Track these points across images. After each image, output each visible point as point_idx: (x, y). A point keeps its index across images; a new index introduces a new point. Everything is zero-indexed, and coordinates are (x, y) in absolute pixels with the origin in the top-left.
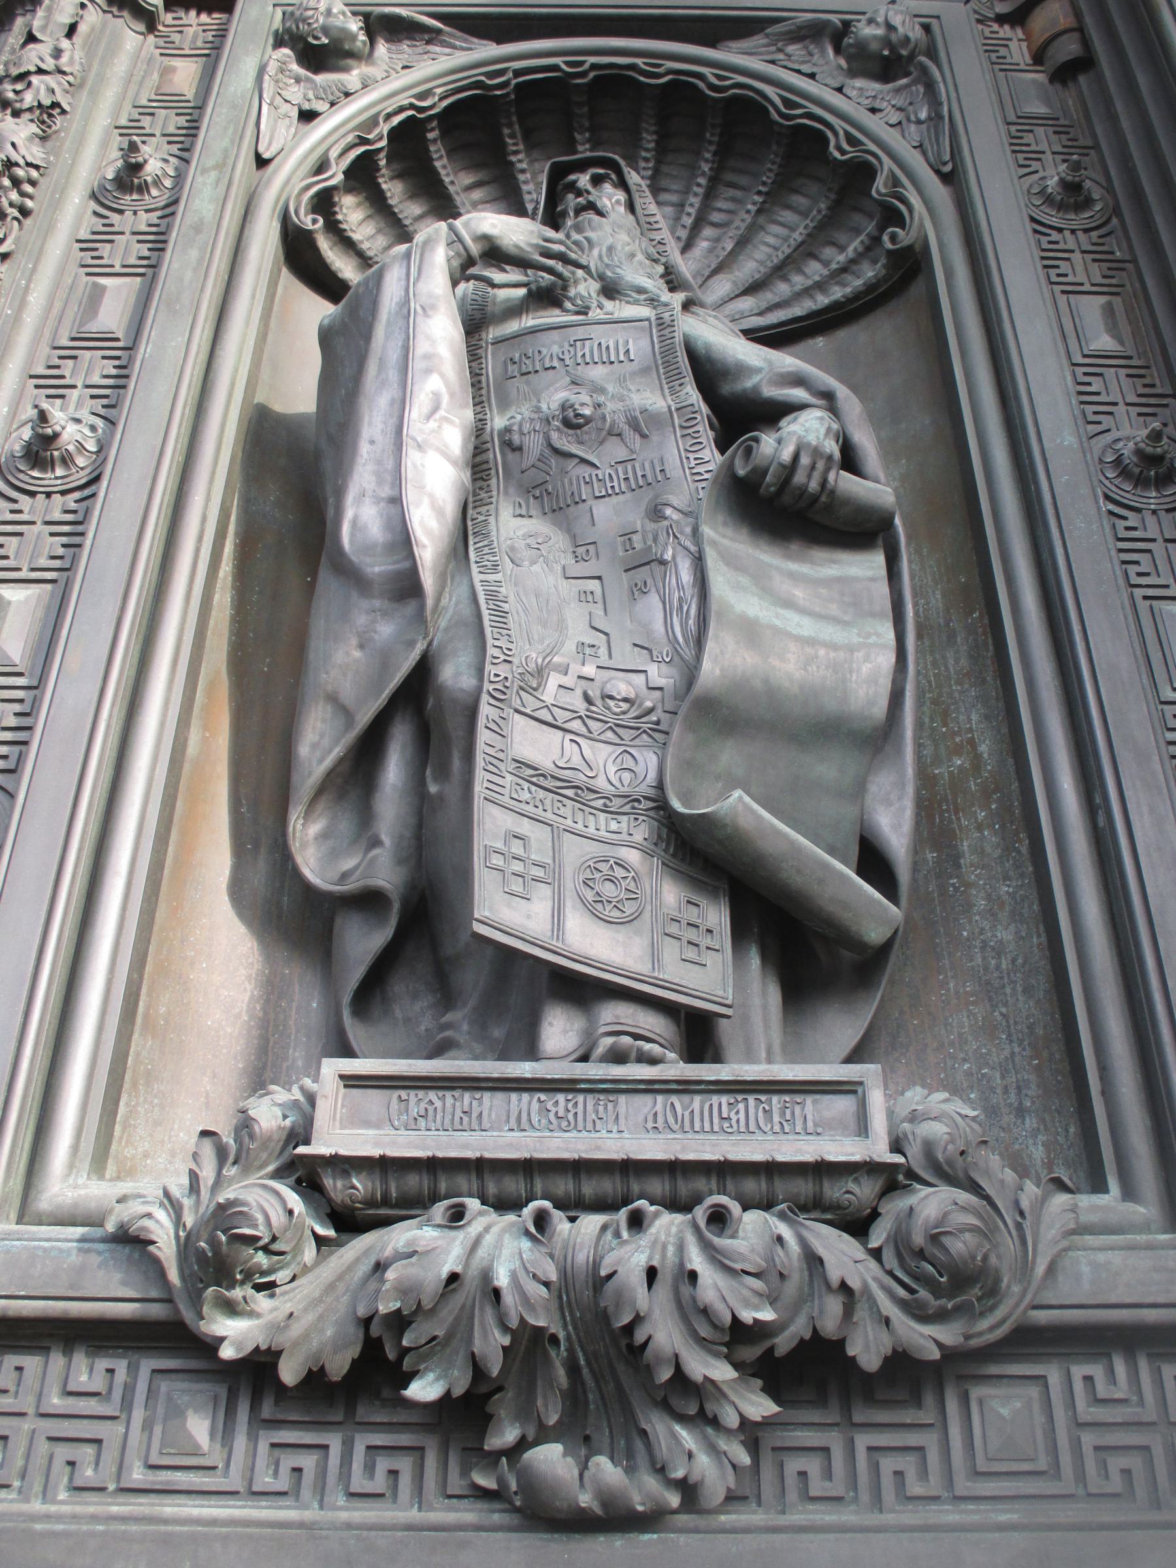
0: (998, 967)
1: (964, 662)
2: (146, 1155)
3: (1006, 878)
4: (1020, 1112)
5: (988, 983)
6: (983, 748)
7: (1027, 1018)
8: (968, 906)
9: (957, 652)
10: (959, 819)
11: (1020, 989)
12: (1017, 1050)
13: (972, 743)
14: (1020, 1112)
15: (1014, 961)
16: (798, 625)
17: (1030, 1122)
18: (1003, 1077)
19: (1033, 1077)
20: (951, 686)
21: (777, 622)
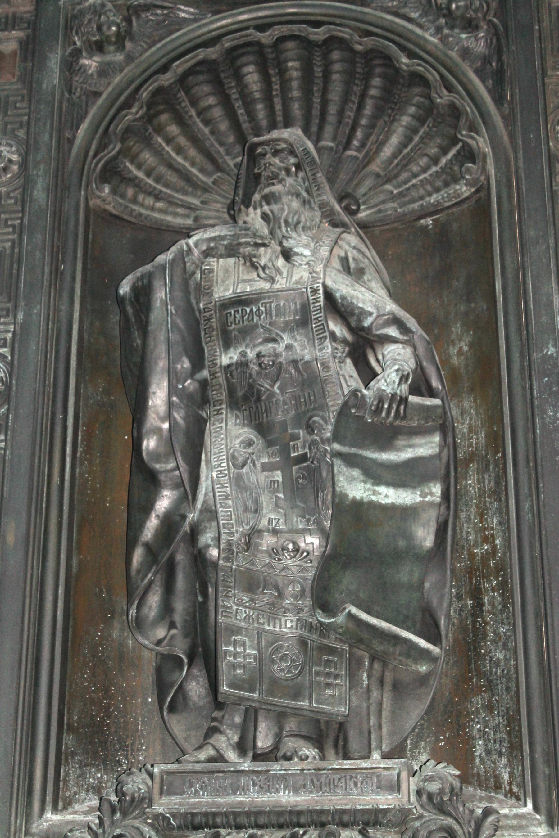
0: (496, 672)
1: (492, 484)
2: (75, 794)
3: (503, 623)
4: (500, 754)
5: (491, 681)
6: (497, 542)
7: (507, 704)
8: (485, 635)
9: (490, 476)
10: (484, 583)
11: (504, 688)
12: (501, 721)
13: (492, 535)
14: (500, 754)
15: (503, 671)
16: (386, 496)
17: (504, 760)
18: (494, 734)
19: (506, 737)
20: (485, 498)
21: (374, 498)
